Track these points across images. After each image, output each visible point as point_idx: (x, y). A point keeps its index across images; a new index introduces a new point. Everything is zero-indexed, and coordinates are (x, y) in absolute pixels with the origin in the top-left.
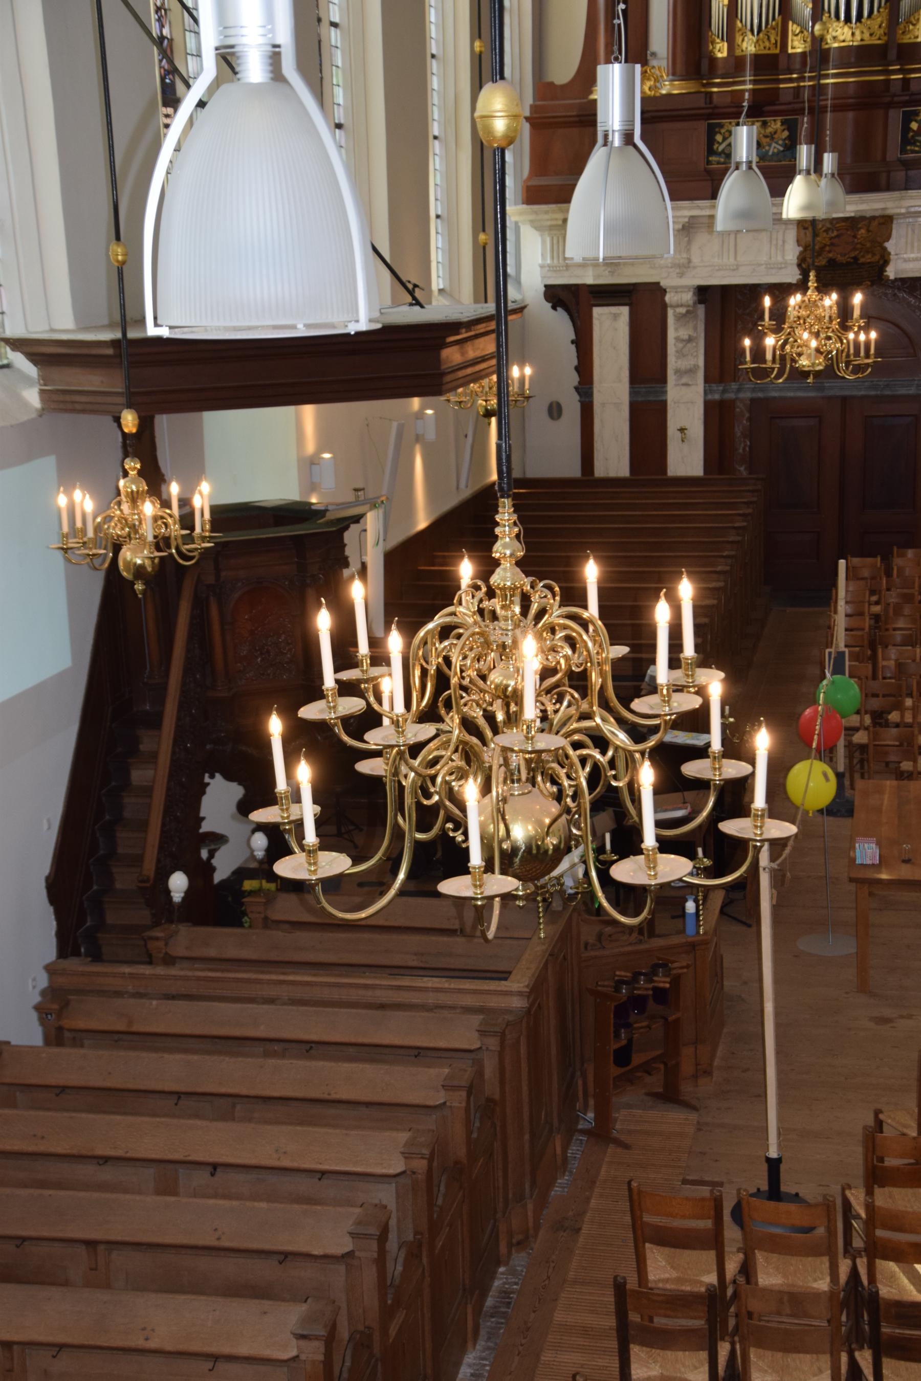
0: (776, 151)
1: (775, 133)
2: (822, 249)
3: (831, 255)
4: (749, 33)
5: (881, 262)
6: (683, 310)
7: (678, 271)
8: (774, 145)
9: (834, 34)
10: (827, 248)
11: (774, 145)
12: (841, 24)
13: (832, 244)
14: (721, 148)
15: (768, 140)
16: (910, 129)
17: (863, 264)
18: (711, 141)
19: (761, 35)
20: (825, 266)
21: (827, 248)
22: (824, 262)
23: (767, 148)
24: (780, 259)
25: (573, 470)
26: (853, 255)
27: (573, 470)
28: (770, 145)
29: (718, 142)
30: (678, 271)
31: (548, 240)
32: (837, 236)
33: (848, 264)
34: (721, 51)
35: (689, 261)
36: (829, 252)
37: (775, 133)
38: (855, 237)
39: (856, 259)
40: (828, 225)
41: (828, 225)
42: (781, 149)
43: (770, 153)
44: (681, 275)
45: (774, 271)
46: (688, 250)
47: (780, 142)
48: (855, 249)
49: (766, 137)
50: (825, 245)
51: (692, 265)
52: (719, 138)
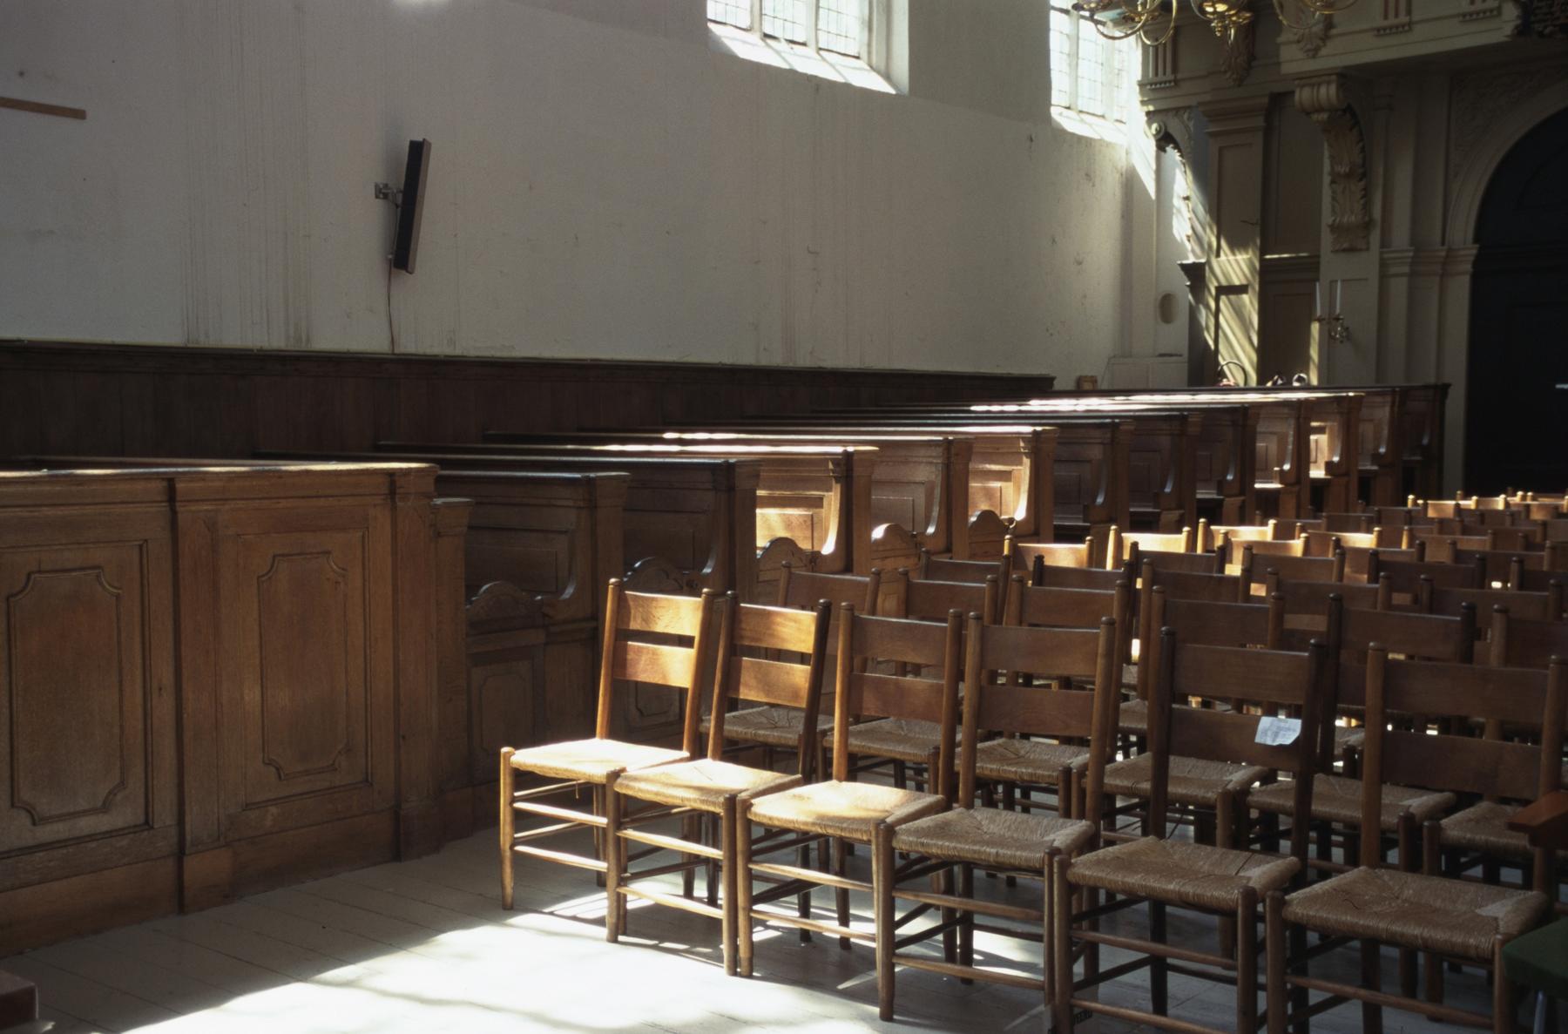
6: (1324, 116)
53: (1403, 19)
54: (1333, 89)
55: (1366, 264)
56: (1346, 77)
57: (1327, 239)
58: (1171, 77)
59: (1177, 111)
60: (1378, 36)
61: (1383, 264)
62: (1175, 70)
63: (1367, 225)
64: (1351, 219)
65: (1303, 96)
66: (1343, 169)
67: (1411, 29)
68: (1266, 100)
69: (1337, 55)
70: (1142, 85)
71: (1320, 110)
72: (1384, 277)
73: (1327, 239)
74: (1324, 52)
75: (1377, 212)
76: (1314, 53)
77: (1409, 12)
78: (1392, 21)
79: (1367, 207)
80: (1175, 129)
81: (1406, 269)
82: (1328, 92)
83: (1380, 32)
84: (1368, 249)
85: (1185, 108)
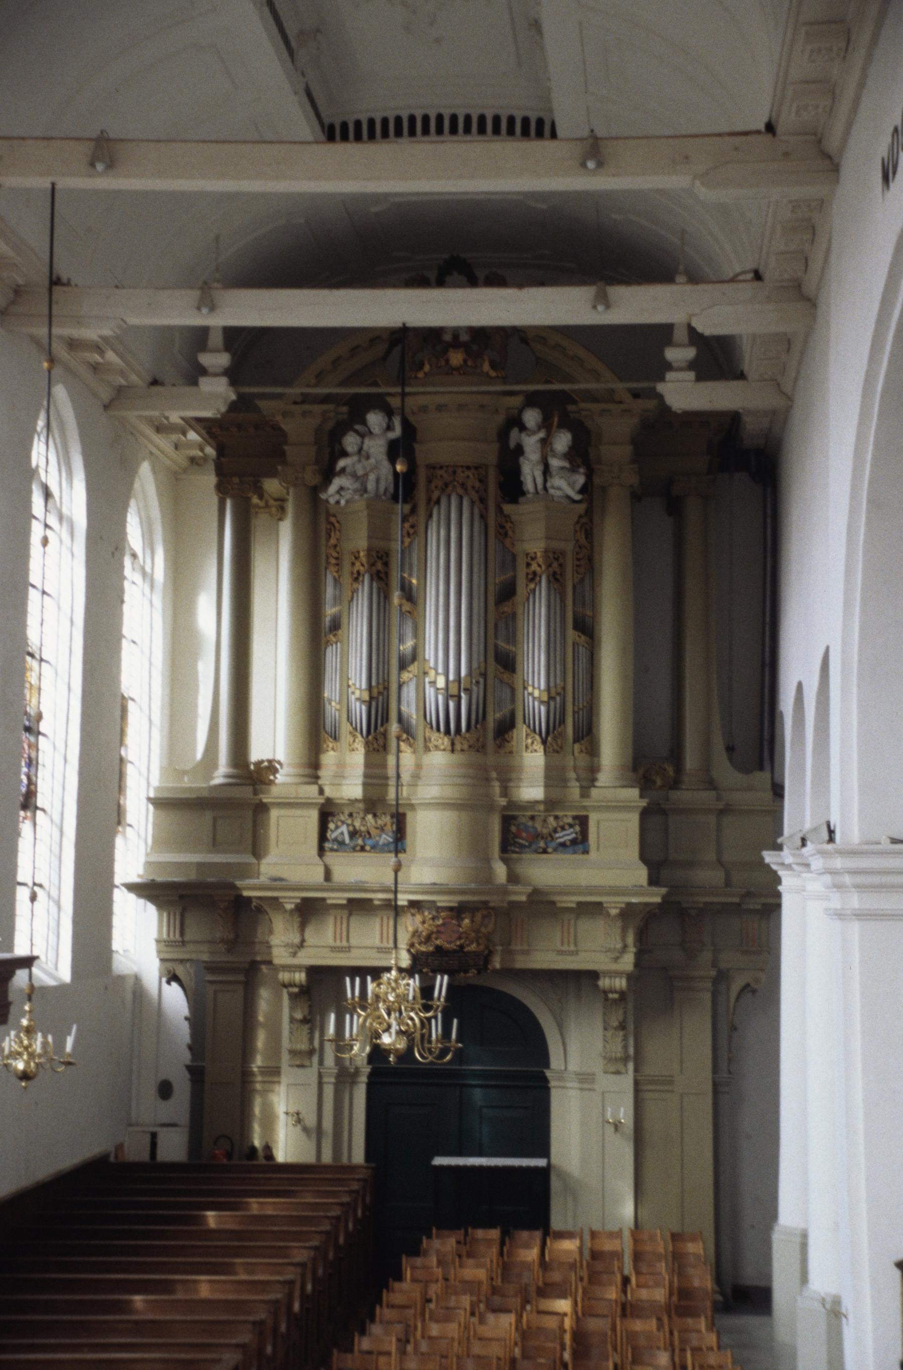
1: (385, 825)
3: (438, 942)
4: (359, 735)
5: (486, 952)
6: (296, 990)
7: (291, 950)
8: (384, 836)
9: (436, 743)
10: (434, 936)
11: (384, 836)
12: (442, 735)
13: (439, 932)
14: (334, 835)
15: (378, 831)
16: (509, 831)
17: (469, 952)
19: (370, 737)
22: (431, 949)
23: (377, 838)
25: (145, 1157)
26: (458, 943)
27: (145, 1157)
28: (380, 836)
30: (291, 950)
31: (165, 915)
32: (443, 925)
33: (454, 951)
35: (303, 941)
36: (436, 939)
37: (385, 825)
38: (459, 926)
39: (461, 947)
47: (391, 834)
48: (460, 938)
49: (377, 828)
50: (432, 933)
51: (305, 944)
52: (332, 826)
53: (345, 943)
55: (311, 1074)
56: (314, 972)
57: (285, 1057)
58: (180, 939)
59: (182, 961)
60: (332, 951)
61: (320, 1076)
62: (182, 934)
63: (311, 1052)
64: (304, 1046)
65: (284, 976)
66: (299, 1015)
67: (350, 951)
68: (247, 966)
69: (308, 958)
70: (158, 941)
71: (295, 985)
72: (320, 1084)
73: (285, 1057)
74: (299, 954)
75: (316, 1044)
76: (294, 954)
77: (348, 940)
78: (338, 944)
79: (311, 1040)
80: (180, 971)
81: (333, 1080)
82: (300, 977)
83: (333, 949)
84: (311, 1066)
85: (188, 960)
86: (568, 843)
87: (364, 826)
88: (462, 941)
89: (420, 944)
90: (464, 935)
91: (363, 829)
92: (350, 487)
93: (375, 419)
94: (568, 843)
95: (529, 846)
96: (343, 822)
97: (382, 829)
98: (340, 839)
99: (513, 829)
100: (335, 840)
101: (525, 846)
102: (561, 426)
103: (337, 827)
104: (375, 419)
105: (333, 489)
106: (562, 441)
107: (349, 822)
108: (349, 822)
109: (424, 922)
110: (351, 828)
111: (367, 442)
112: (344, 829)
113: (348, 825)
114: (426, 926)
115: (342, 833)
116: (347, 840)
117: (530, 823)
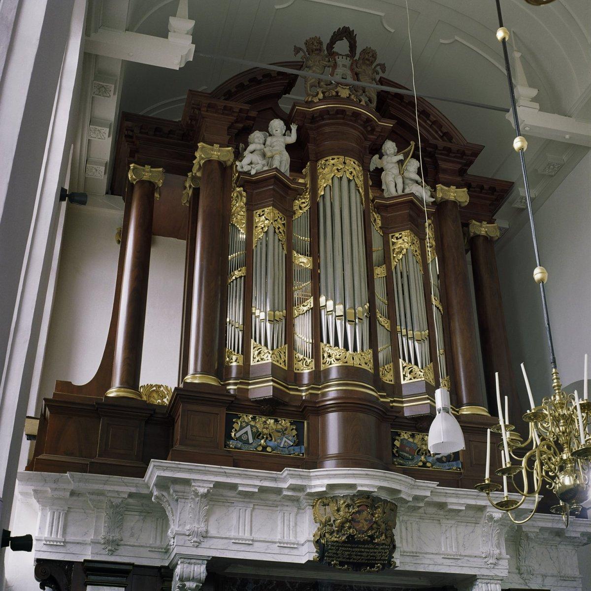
0: (286, 444)
2: (342, 526)
8: (285, 439)
11: (285, 439)
14: (238, 435)
15: (279, 434)
17: (378, 544)
18: (229, 427)
20: (344, 542)
21: (348, 525)
22: (344, 538)
23: (279, 441)
24: (292, 539)
26: (370, 533)
28: (282, 440)
29: (236, 430)
31: (49, 514)
33: (365, 542)
34: (235, 361)
36: (350, 528)
38: (373, 515)
39: (372, 537)
40: (349, 501)
41: (349, 501)
42: (292, 444)
43: (282, 446)
44: (198, 545)
45: (286, 551)
46: (207, 521)
48: (371, 528)
49: (279, 432)
54: (203, 568)
74: (203, 545)
86: (444, 459)
87: (267, 428)
88: (373, 531)
89: (331, 533)
90: (375, 526)
91: (265, 431)
92: (260, 162)
93: (277, 125)
94: (444, 459)
95: (412, 459)
96: (247, 424)
97: (283, 432)
98: (244, 438)
99: (397, 443)
100: (239, 439)
101: (409, 459)
102: (415, 156)
103: (242, 428)
104: (277, 125)
105: (246, 161)
106: (413, 166)
107: (252, 423)
108: (252, 423)
109: (338, 510)
110: (254, 430)
111: (269, 139)
112: (248, 428)
113: (252, 427)
114: (341, 513)
115: (246, 433)
116: (251, 441)
117: (411, 440)
